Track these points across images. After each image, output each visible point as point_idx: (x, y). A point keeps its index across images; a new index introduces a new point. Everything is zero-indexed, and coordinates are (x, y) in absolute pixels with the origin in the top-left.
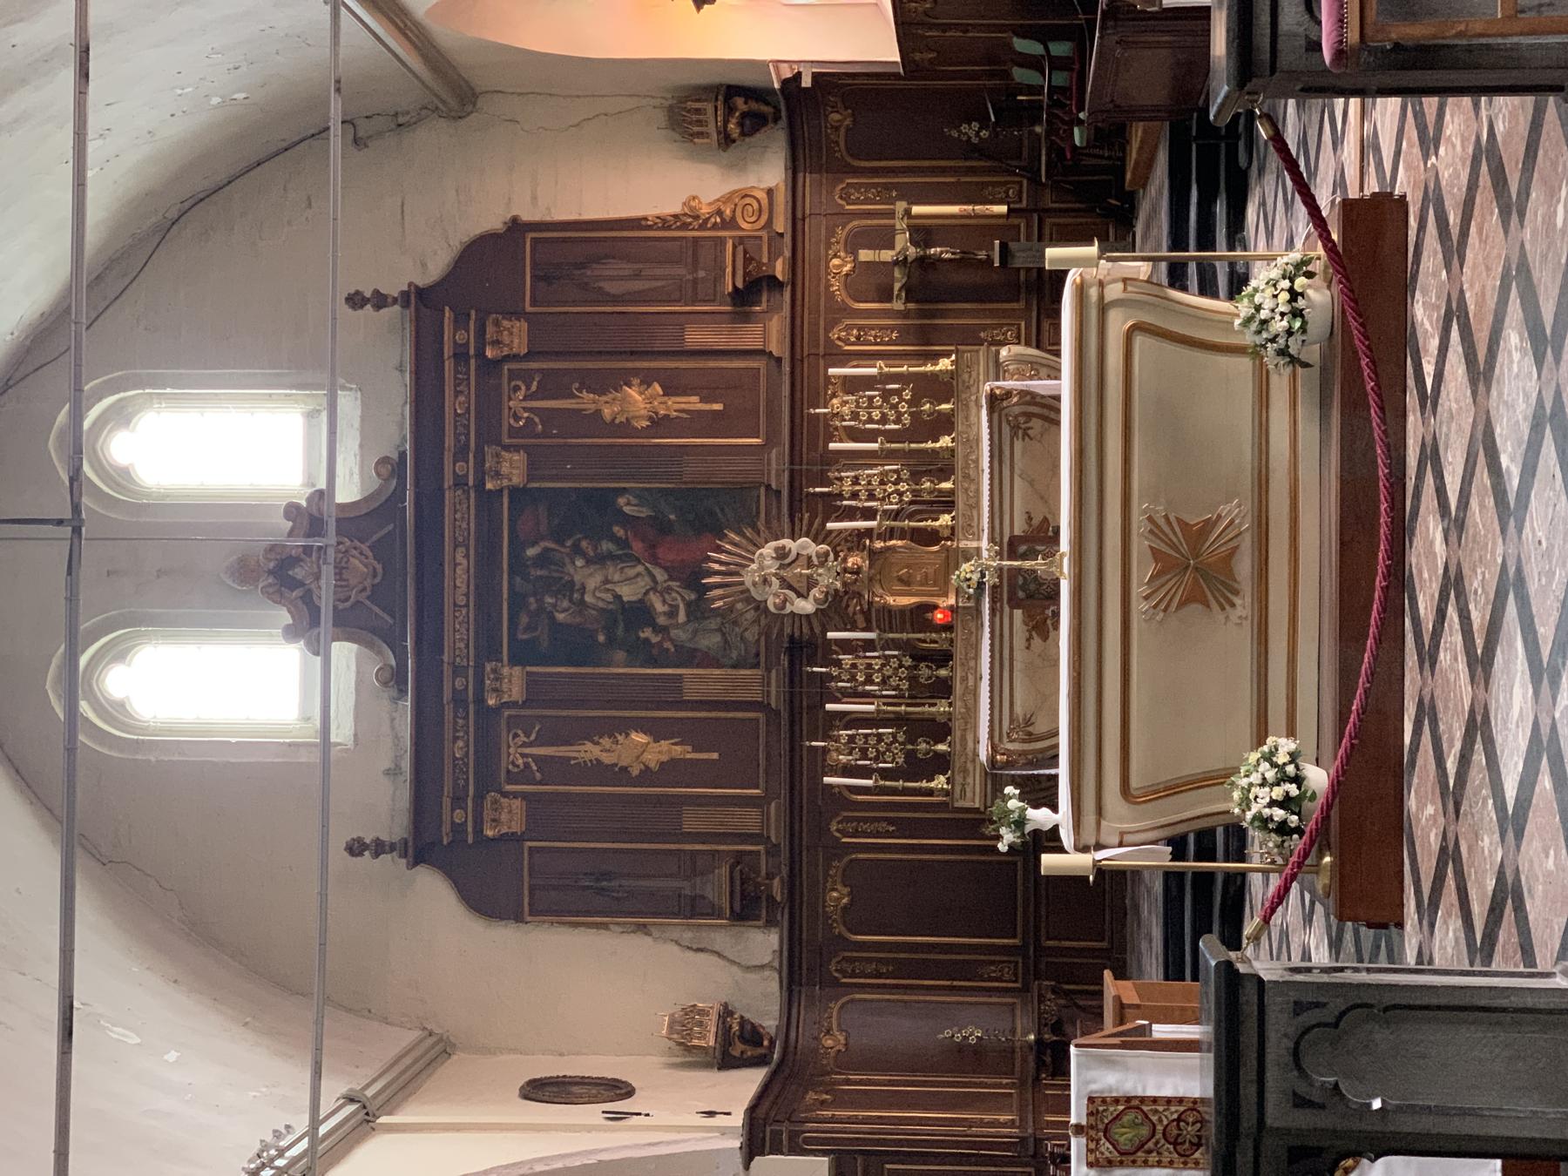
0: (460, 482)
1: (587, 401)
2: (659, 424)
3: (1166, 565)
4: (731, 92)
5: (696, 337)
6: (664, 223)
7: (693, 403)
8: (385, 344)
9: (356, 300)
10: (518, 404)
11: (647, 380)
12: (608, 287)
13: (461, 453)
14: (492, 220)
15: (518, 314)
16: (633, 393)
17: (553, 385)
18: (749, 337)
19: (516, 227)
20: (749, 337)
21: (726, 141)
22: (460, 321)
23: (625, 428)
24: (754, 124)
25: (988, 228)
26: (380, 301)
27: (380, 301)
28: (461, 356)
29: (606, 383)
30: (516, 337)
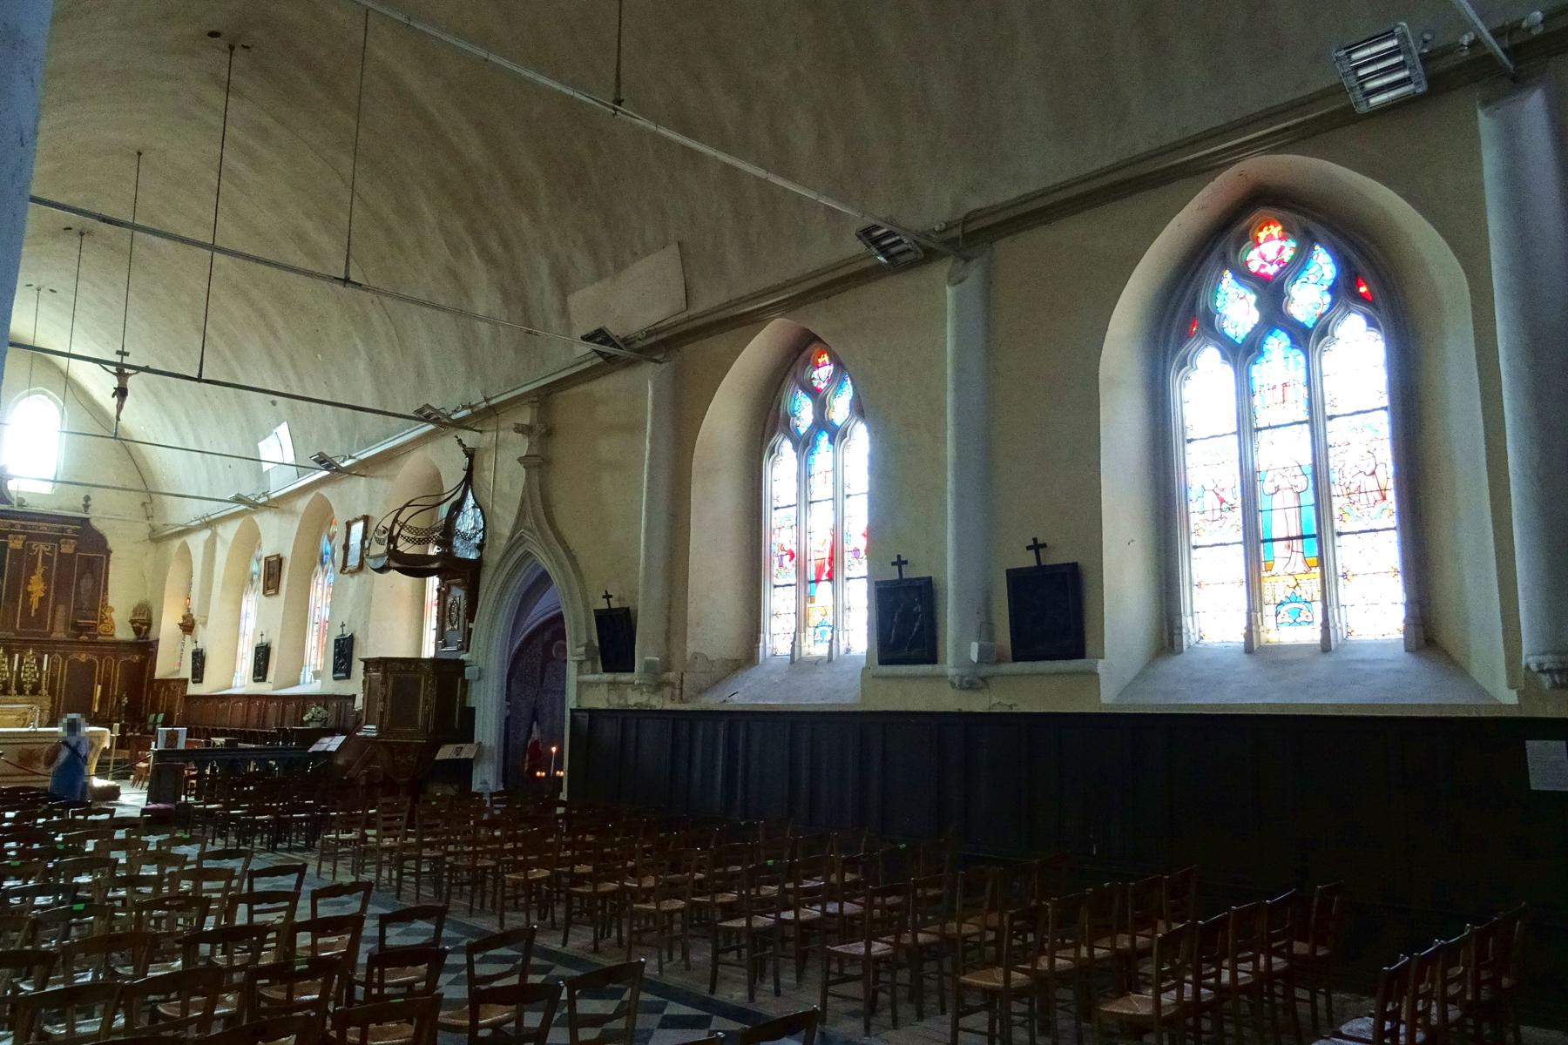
0: (12, 526)
1: (40, 570)
2: (28, 595)
3: (31, 752)
4: (149, 625)
5: (61, 609)
6: (105, 600)
7: (35, 605)
8: (68, 504)
9: (87, 498)
10: (41, 548)
11: (47, 592)
12: (83, 583)
13: (23, 527)
14: (112, 543)
15: (76, 549)
16: (42, 586)
17: (47, 560)
18: (59, 626)
19: (109, 552)
20: (59, 626)
21: (133, 622)
22: (75, 531)
23: (28, 583)
24: (137, 631)
25: (91, 705)
26: (86, 507)
27: (86, 507)
28: (63, 530)
29: (46, 577)
30: (67, 549)
